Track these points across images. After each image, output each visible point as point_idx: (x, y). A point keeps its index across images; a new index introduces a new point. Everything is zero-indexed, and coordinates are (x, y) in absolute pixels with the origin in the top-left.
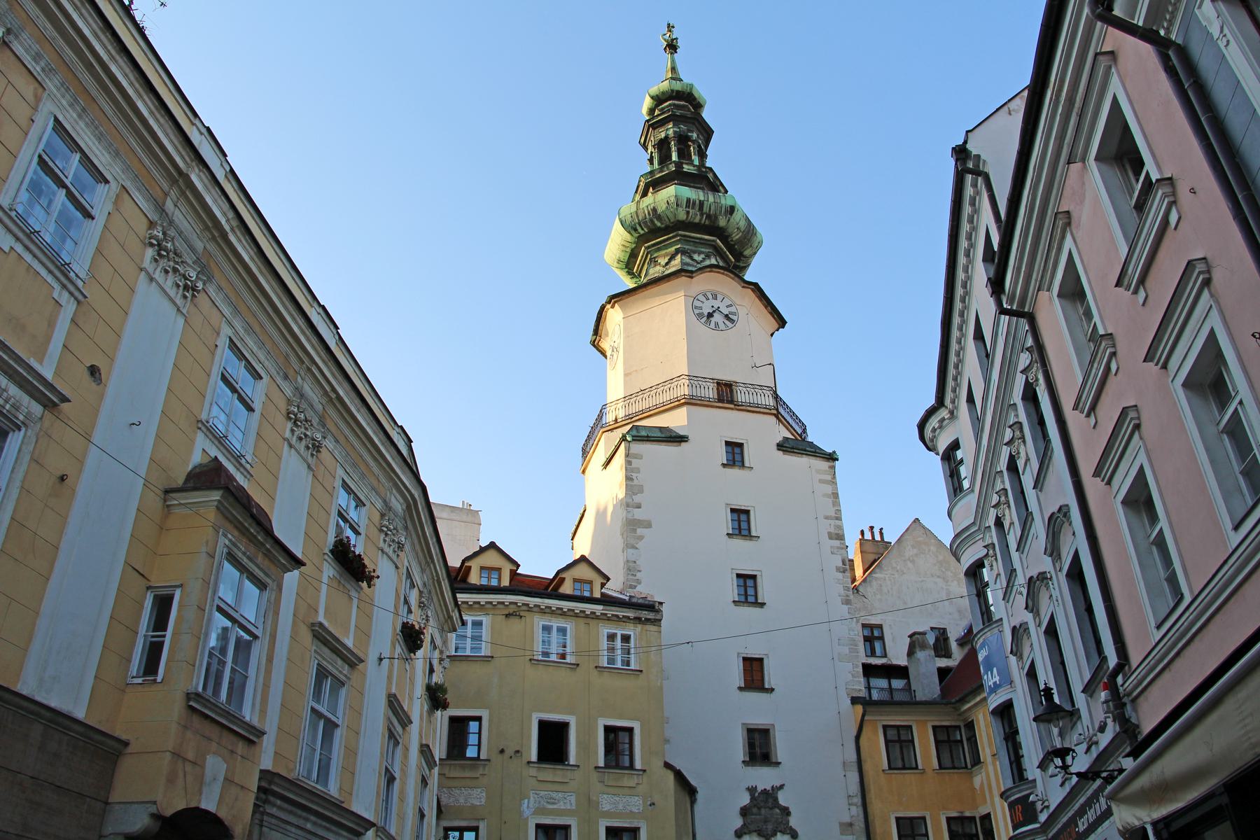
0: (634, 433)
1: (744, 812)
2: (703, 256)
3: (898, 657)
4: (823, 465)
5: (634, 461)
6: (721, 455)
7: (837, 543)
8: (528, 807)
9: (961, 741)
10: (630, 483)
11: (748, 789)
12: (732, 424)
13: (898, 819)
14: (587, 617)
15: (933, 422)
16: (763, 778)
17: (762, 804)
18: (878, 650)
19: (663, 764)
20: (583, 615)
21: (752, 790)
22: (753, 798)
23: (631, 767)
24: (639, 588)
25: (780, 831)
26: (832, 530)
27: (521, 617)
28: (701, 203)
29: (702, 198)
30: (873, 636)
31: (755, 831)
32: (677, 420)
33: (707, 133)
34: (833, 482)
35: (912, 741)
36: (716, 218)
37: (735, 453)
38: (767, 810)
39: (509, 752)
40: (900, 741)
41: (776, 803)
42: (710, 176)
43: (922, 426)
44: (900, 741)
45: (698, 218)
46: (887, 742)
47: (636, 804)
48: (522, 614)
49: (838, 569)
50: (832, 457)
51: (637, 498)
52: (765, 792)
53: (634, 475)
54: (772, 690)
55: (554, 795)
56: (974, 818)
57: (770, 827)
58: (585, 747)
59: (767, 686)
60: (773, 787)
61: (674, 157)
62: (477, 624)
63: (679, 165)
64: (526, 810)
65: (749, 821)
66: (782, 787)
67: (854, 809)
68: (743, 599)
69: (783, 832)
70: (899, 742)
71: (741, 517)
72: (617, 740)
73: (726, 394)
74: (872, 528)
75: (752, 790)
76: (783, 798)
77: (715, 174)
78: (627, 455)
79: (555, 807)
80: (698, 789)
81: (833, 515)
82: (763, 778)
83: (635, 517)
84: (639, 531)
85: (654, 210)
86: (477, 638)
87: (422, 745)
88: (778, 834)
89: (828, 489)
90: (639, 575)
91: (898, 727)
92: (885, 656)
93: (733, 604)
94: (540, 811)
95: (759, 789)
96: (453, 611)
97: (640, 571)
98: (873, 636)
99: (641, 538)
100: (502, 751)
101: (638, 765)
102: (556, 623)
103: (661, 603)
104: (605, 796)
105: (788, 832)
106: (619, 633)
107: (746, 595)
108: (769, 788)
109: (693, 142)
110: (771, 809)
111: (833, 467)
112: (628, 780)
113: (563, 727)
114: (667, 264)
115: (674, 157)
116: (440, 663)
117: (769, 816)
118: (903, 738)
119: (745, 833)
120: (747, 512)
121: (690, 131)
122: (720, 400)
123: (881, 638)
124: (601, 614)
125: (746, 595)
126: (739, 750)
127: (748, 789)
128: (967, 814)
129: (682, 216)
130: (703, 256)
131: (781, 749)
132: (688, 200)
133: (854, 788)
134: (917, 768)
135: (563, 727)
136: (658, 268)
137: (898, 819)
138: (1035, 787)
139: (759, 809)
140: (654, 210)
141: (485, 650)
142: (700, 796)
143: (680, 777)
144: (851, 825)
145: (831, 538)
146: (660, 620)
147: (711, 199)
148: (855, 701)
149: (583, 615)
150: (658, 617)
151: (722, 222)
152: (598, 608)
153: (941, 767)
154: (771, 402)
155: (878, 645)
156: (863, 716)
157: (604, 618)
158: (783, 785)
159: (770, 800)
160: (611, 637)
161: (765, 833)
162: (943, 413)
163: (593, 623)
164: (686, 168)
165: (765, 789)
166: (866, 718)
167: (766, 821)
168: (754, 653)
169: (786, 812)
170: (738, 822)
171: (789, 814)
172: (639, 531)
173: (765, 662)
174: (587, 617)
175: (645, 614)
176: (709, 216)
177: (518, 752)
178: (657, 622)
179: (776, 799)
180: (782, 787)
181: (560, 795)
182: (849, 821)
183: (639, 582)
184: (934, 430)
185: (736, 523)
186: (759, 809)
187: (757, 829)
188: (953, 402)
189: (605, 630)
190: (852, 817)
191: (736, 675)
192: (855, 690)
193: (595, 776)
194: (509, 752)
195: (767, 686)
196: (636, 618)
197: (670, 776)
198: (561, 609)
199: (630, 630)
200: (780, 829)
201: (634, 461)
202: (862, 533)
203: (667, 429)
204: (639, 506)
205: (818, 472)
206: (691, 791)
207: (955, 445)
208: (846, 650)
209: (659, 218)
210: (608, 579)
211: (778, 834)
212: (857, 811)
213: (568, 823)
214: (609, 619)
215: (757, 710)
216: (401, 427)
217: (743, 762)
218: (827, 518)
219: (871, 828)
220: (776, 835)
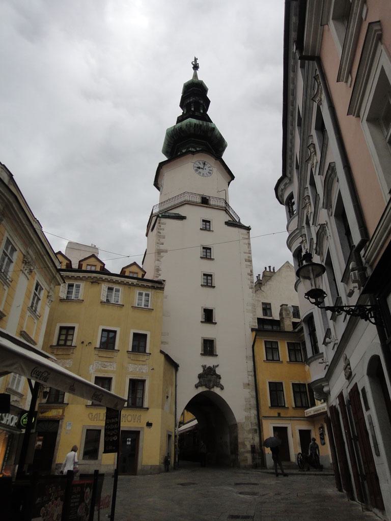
0: (163, 214)
1: (200, 376)
3: (276, 316)
4: (245, 231)
5: (162, 225)
6: (200, 225)
7: (249, 263)
8: (92, 368)
9: (300, 350)
10: (159, 234)
11: (202, 366)
12: (206, 213)
13: (270, 383)
14: (130, 285)
15: (282, 186)
16: (210, 362)
18: (268, 313)
19: (159, 351)
20: (127, 284)
21: (204, 367)
22: (204, 370)
23: (145, 351)
24: (159, 277)
25: (216, 386)
26: (247, 258)
27: (99, 283)
28: (201, 126)
29: (201, 124)
30: (267, 308)
32: (181, 211)
33: (208, 102)
34: (249, 238)
35: (278, 348)
37: (206, 225)
39: (86, 343)
40: (272, 348)
41: (215, 373)
43: (276, 189)
44: (272, 348)
45: (199, 132)
46: (266, 348)
47: (145, 369)
48: (99, 282)
49: (248, 274)
50: (248, 229)
51: (162, 240)
52: (210, 368)
53: (161, 231)
54: (216, 323)
55: (106, 364)
56: (305, 384)
57: (211, 385)
59: (214, 322)
61: (193, 109)
62: (78, 286)
63: (194, 112)
64: (91, 370)
66: (218, 366)
67: (250, 377)
68: (206, 284)
69: (217, 387)
70: (272, 349)
71: (207, 249)
72: (140, 340)
73: (205, 201)
74: (270, 267)
75: (204, 367)
76: (218, 371)
78: (159, 223)
79: (106, 369)
80: (180, 365)
81: (248, 252)
82: (210, 362)
83: (161, 248)
84: (161, 254)
86: (77, 292)
87: (21, 332)
88: (215, 387)
89: (246, 241)
90: (160, 272)
91: (272, 342)
92: (272, 316)
93: (201, 286)
94: (99, 371)
95: (207, 366)
96: (56, 274)
97: (161, 270)
98: (267, 308)
99: (162, 257)
100: (83, 343)
101: (148, 351)
103: (164, 281)
104: (130, 365)
107: (207, 283)
108: (212, 366)
109: (201, 104)
110: (212, 375)
111: (249, 233)
112: (142, 357)
115: (193, 109)
116: (48, 298)
118: (273, 347)
120: (210, 249)
122: (202, 203)
123: (270, 309)
124: (137, 284)
125: (207, 283)
126: (199, 348)
127: (202, 366)
128: (302, 382)
131: (219, 348)
132: (195, 124)
133: (251, 368)
134: (279, 360)
137: (270, 383)
138: (323, 357)
139: (207, 375)
140: (181, 128)
141: (81, 297)
142: (180, 369)
143: (168, 358)
144: (249, 384)
145: (246, 261)
146: (163, 288)
147: (205, 124)
148: (253, 330)
149: (127, 284)
150: (162, 287)
151: (209, 135)
152: (135, 281)
153: (290, 361)
154: (224, 205)
155: (268, 311)
156: (256, 336)
157: (137, 286)
160: (140, 294)
162: (286, 181)
163: (132, 288)
164: (197, 114)
166: (257, 337)
167: (210, 381)
168: (209, 307)
169: (219, 377)
170: (197, 381)
171: (220, 378)
172: (161, 254)
173: (214, 311)
174: (130, 285)
175: (156, 285)
177: (90, 343)
178: (162, 289)
179: (215, 371)
180: (218, 366)
181: (109, 364)
182: (248, 382)
183: (160, 275)
184: (282, 190)
185: (205, 254)
188: (290, 173)
189: (137, 291)
190: (249, 381)
191: (200, 316)
192: (254, 326)
194: (86, 343)
195: (214, 322)
196: (152, 286)
197: (162, 357)
198: (118, 281)
199: (150, 292)
201: (162, 225)
202: (266, 268)
203: (178, 214)
204: (163, 244)
205: (242, 234)
206: (175, 366)
207: (291, 196)
208: (250, 308)
210: (145, 273)
211: (215, 387)
212: (251, 379)
213: (112, 376)
214: (140, 286)
215: (209, 331)
216: (4, 165)
217: (201, 354)
218: (245, 253)
219: (258, 386)
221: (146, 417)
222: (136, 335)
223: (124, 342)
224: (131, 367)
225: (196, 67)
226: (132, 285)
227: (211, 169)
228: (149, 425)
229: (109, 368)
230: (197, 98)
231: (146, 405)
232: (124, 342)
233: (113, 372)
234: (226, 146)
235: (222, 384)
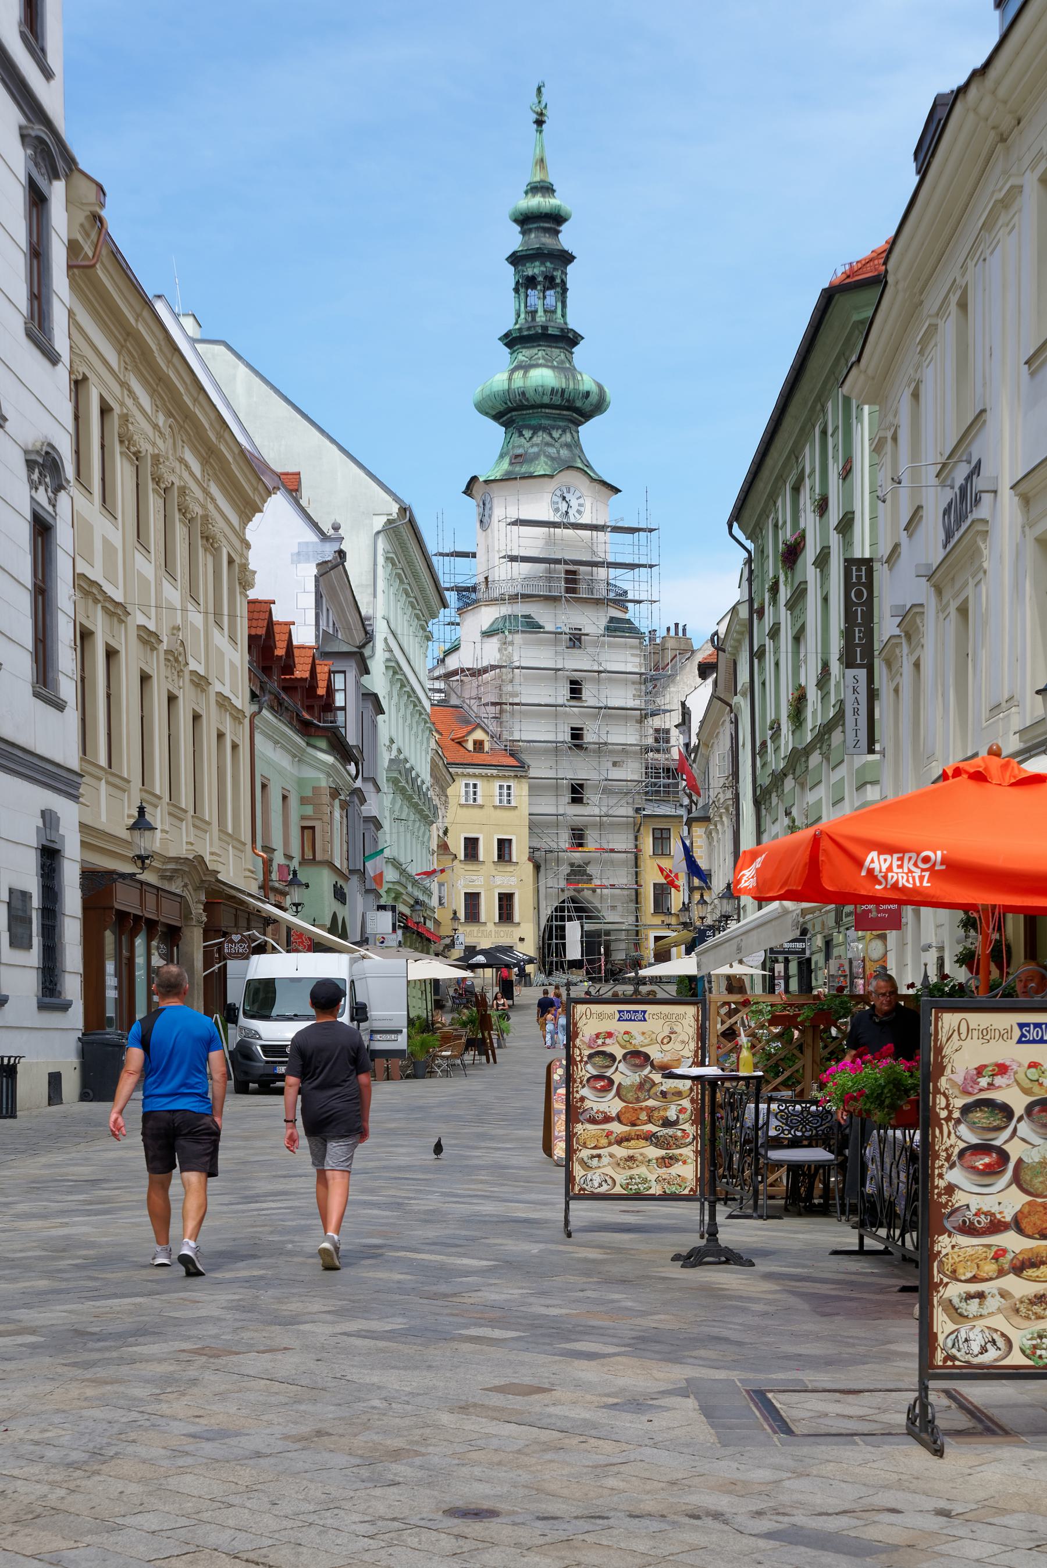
2: (560, 432)
20: (487, 776)
28: (563, 391)
36: (574, 401)
42: (571, 335)
46: (654, 838)
58: (487, 851)
77: (575, 332)
85: (523, 393)
101: (514, 859)
102: (471, 782)
106: (505, 784)
112: (510, 868)
113: (476, 840)
114: (531, 438)
121: (555, 269)
129: (546, 400)
130: (560, 432)
135: (476, 840)
136: (522, 440)
140: (523, 393)
151: (578, 404)
157: (498, 777)
176: (568, 401)
189: (497, 784)
193: (492, 866)
202: (668, 629)
209: (527, 400)
221: (518, 933)
222: (501, 842)
223: (488, 850)
224: (498, 880)
225: (540, 123)
226: (492, 776)
227: (581, 501)
228: (522, 940)
229: (476, 883)
230: (548, 264)
231: (517, 918)
232: (488, 850)
233: (480, 886)
234: (608, 406)
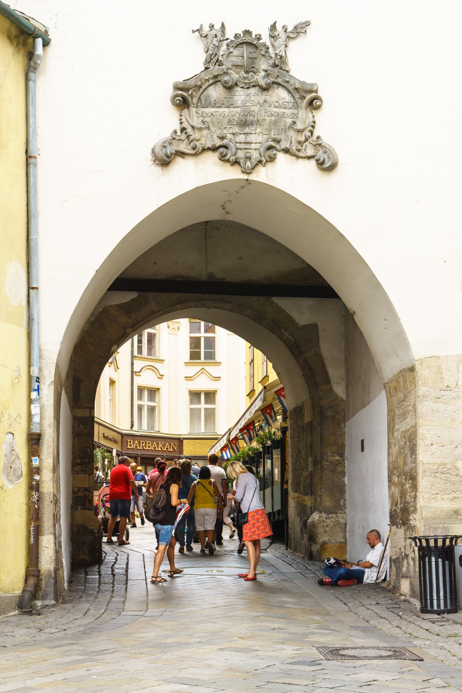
17: (235, 76)
25: (286, 151)
31: (214, 149)
38: (253, 91)
60: (273, 27)
65: (196, 122)
105: (310, 151)
117: (256, 109)
119: (182, 154)
139: (229, 88)
158: (307, 24)
159: (263, 65)
161: (241, 154)
165: (247, 32)
186: (229, 88)
187: (218, 143)
200: (284, 145)
211: (281, 156)
220: (272, 159)
235: (326, 140)
